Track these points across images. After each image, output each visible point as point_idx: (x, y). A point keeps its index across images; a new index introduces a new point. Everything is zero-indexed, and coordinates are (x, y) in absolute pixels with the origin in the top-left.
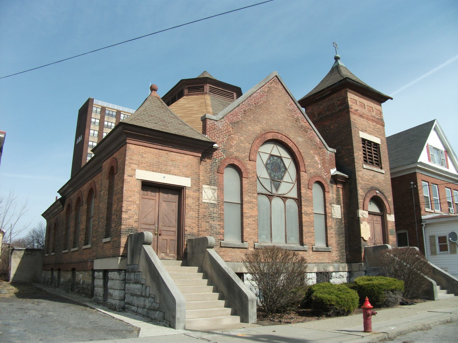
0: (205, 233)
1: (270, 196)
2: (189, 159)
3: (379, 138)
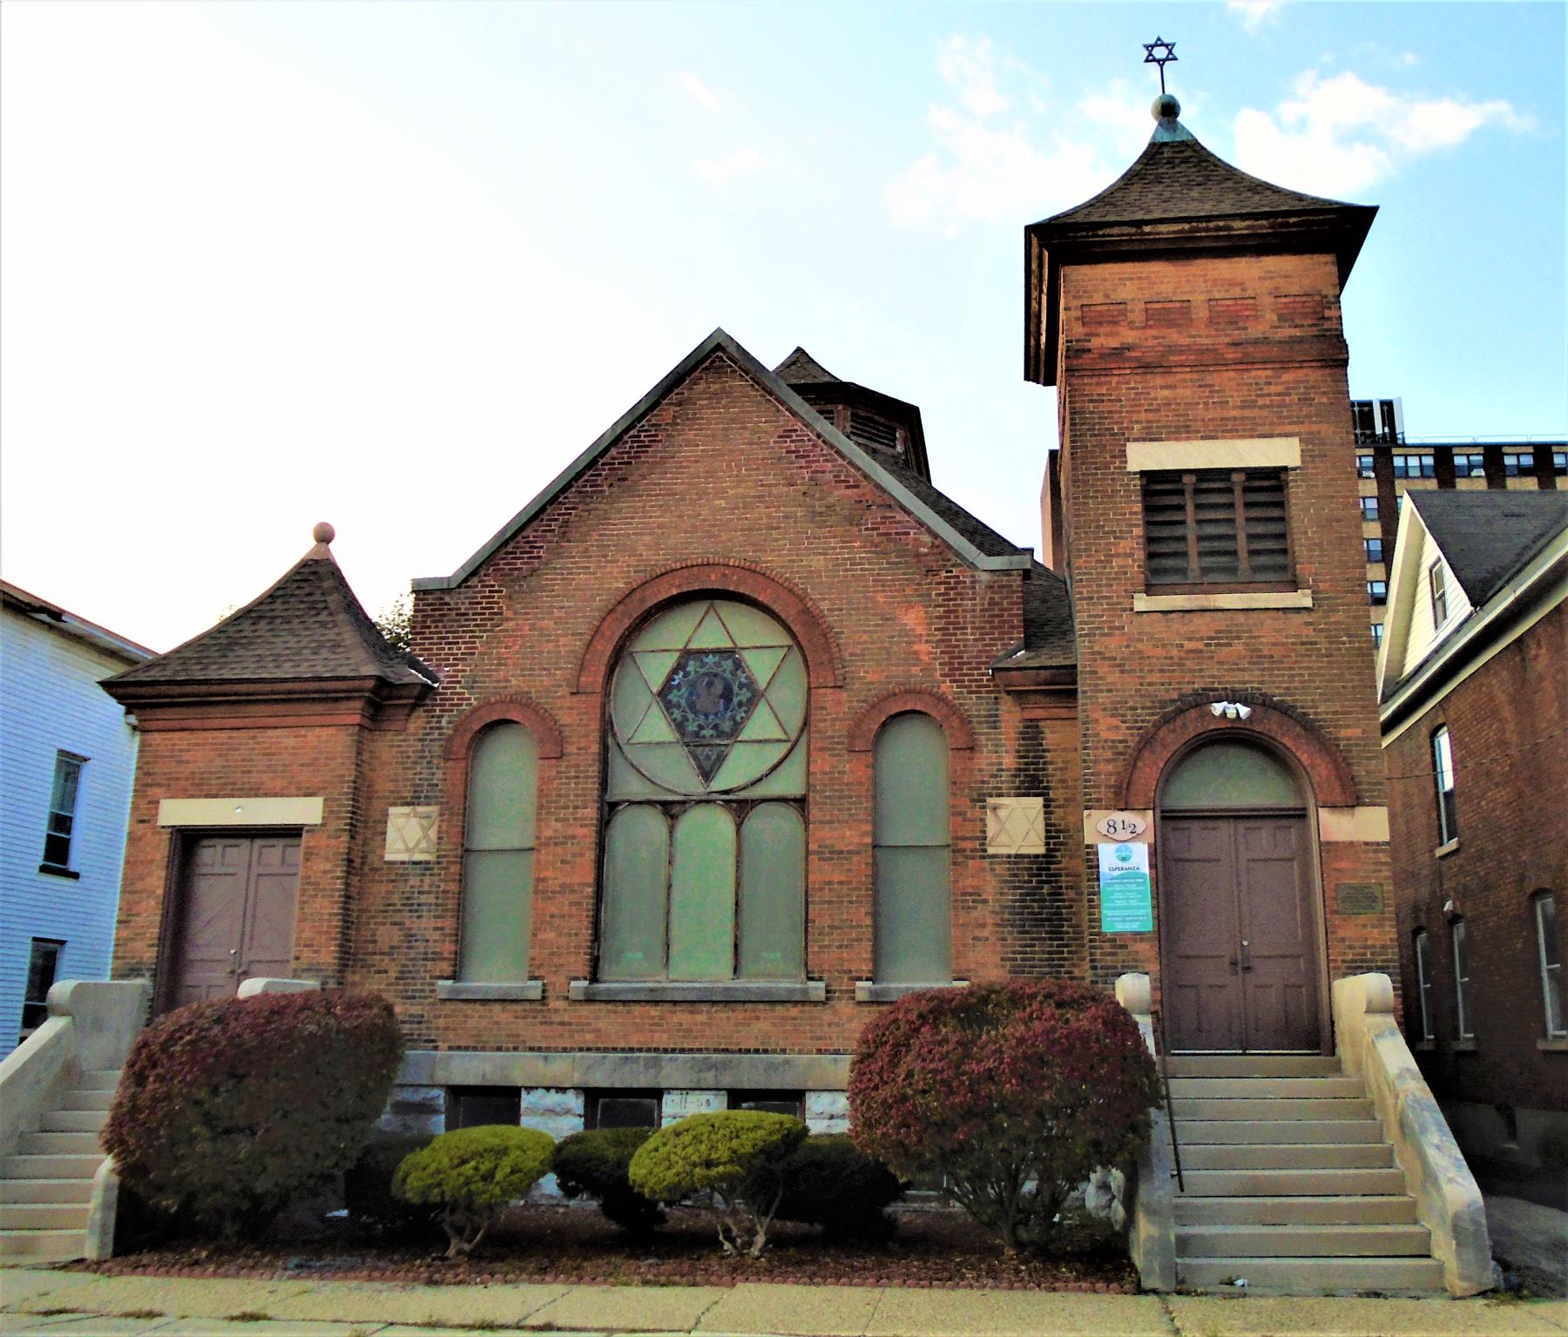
0: (386, 959)
1: (671, 810)
2: (327, 739)
3: (1286, 435)
